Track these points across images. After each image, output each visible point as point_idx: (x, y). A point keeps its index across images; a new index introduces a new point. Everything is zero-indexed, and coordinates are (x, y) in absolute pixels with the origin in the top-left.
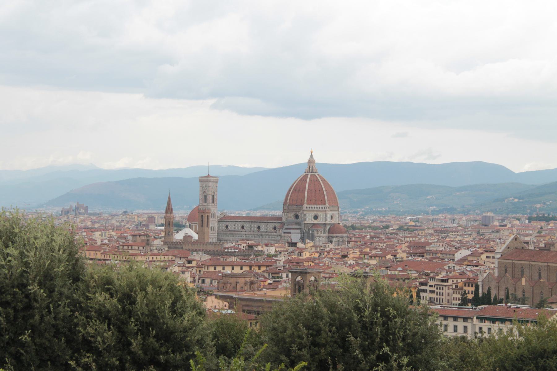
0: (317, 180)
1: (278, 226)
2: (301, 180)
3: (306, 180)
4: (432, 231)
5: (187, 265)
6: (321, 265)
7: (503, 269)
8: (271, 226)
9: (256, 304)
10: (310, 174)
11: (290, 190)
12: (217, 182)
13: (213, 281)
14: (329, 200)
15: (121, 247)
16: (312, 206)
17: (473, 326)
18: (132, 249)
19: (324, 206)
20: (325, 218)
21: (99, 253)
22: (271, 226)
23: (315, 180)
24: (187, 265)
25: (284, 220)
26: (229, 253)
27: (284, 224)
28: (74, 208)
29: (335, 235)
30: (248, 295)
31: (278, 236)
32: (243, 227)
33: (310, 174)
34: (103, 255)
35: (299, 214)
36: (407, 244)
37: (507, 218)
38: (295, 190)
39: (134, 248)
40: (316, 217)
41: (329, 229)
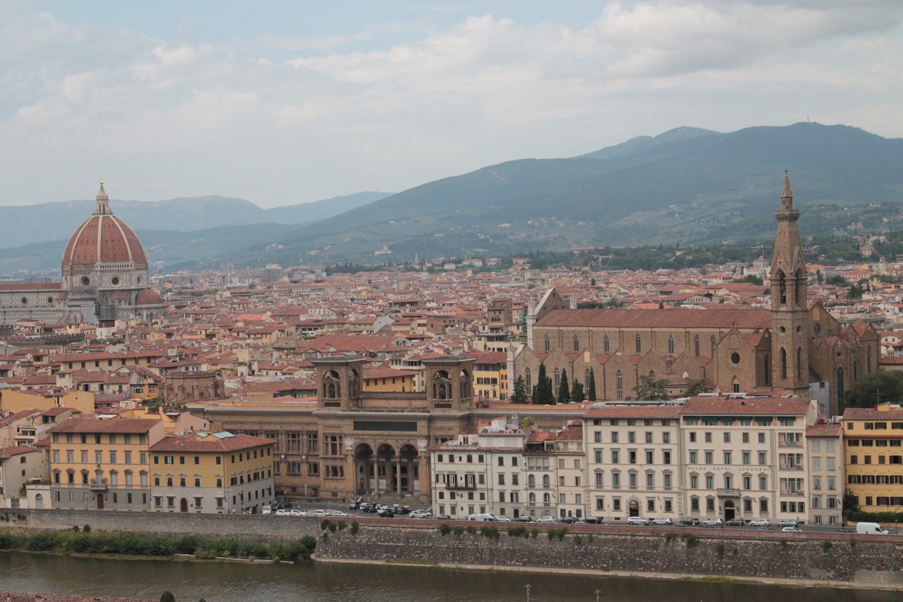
0: (114, 225)
1: (55, 296)
2: (88, 226)
3: (97, 226)
4: (227, 294)
5: (36, 363)
6: (206, 350)
7: (543, 340)
8: (44, 298)
9: (247, 419)
11: (72, 242)
13: (105, 387)
14: (133, 255)
16: (109, 264)
17: (681, 432)
19: (127, 263)
20: (130, 281)
22: (44, 298)
23: (109, 225)
25: (65, 287)
26: (33, 340)
27: (66, 293)
30: (224, 405)
31: (57, 311)
33: (101, 217)
35: (90, 277)
36: (269, 313)
37: (296, 270)
38: (81, 241)
40: (115, 281)
41: (136, 297)
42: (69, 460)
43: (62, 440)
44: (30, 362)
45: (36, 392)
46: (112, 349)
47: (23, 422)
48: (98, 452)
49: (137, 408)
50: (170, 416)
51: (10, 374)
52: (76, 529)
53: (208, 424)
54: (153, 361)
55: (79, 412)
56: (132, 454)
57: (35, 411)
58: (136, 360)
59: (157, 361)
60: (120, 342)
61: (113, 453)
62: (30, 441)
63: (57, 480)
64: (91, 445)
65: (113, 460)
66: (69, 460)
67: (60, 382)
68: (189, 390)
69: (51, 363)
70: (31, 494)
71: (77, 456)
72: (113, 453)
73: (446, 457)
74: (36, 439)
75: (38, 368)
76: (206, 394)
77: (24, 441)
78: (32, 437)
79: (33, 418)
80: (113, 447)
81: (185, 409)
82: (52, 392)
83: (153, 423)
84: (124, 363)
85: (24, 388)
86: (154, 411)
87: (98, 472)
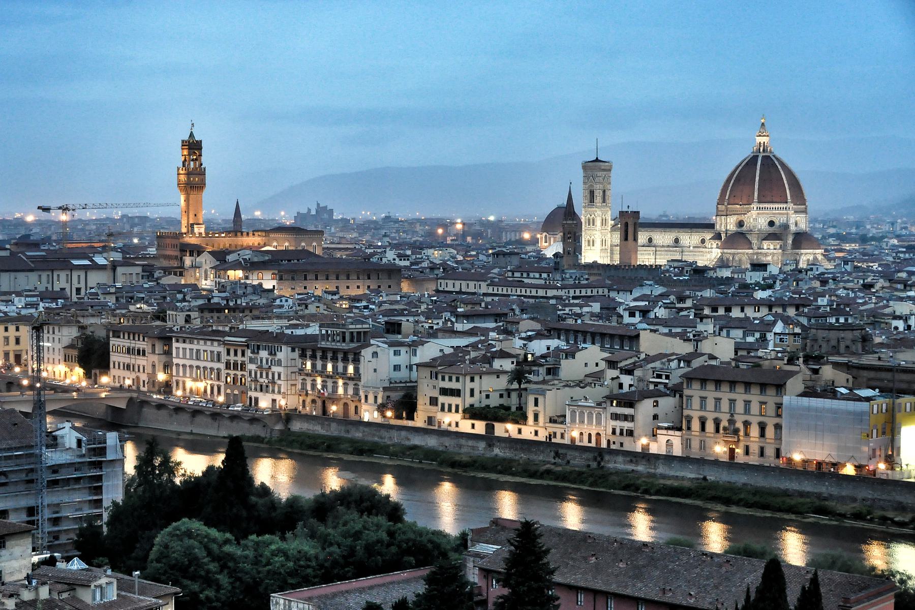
2: (747, 164)
6: (860, 301)
10: (761, 155)
12: (610, 170)
15: (510, 274)
18: (528, 277)
19: (785, 206)
21: (484, 285)
24: (678, 305)
28: (313, 212)
29: (803, 251)
30: (869, 360)
32: (650, 240)
33: (761, 155)
34: (491, 288)
39: (531, 275)
42: (703, 407)
43: (696, 385)
44: (672, 303)
45: (674, 335)
46: (760, 295)
47: (657, 364)
48: (732, 402)
49: (777, 358)
50: (810, 369)
51: (652, 315)
52: (705, 479)
53: (850, 377)
54: (801, 310)
55: (716, 358)
56: (708, 400)
57: (673, 354)
58: (784, 307)
59: (806, 310)
60: (770, 287)
61: (747, 403)
62: (665, 385)
63: (689, 428)
64: (725, 395)
65: (747, 411)
66: (703, 407)
67: (700, 327)
68: (834, 343)
69: (695, 307)
70: (662, 438)
71: (710, 404)
72: (747, 403)
73: (447, 378)
74: (671, 382)
75: (681, 309)
76: (853, 348)
77: (656, 384)
78: (667, 381)
79: (669, 361)
80: (703, 394)
81: (828, 363)
82: (691, 337)
83: (792, 374)
84: (770, 310)
85: (666, 330)
86: (791, 361)
87: (731, 422)
